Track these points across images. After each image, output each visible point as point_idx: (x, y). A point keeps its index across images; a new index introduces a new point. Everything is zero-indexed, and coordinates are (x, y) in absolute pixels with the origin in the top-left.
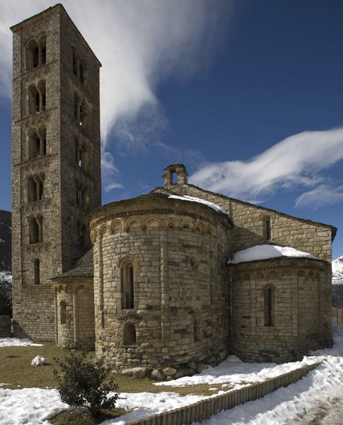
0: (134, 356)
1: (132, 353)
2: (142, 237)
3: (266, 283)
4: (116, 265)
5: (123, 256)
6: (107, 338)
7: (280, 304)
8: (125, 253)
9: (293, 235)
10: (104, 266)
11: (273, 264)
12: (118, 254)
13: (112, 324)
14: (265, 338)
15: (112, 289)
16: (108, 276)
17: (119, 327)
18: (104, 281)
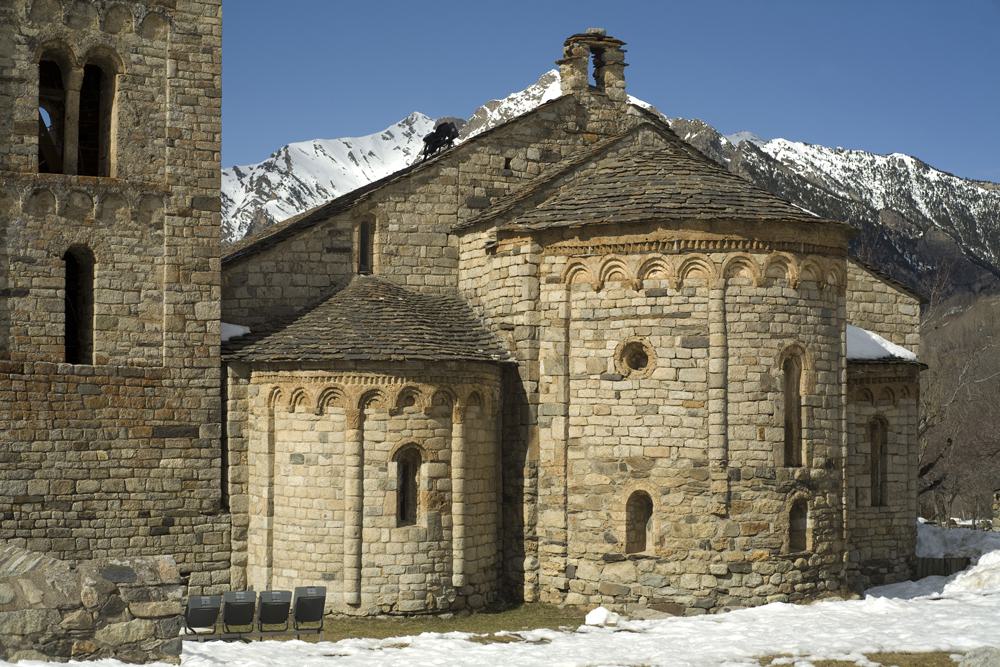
0: (807, 574)
1: (803, 569)
2: (821, 304)
3: (871, 411)
4: (771, 361)
5: (788, 342)
6: (740, 541)
7: (896, 458)
8: (790, 336)
9: (859, 302)
10: (731, 361)
11: (888, 372)
12: (775, 336)
13: (758, 503)
14: (871, 532)
15: (761, 419)
16: (747, 386)
17: (779, 510)
18: (731, 397)
